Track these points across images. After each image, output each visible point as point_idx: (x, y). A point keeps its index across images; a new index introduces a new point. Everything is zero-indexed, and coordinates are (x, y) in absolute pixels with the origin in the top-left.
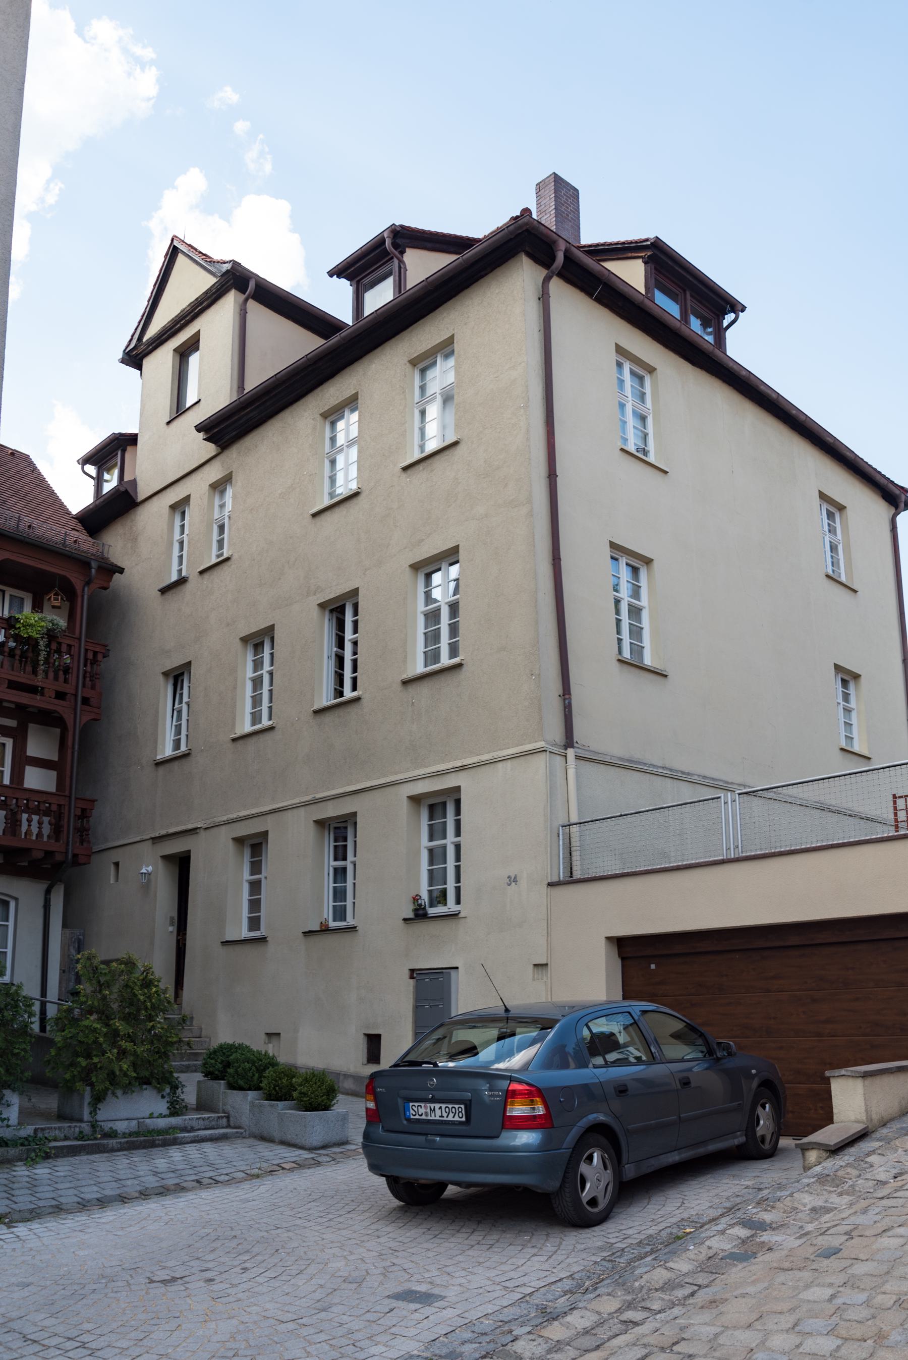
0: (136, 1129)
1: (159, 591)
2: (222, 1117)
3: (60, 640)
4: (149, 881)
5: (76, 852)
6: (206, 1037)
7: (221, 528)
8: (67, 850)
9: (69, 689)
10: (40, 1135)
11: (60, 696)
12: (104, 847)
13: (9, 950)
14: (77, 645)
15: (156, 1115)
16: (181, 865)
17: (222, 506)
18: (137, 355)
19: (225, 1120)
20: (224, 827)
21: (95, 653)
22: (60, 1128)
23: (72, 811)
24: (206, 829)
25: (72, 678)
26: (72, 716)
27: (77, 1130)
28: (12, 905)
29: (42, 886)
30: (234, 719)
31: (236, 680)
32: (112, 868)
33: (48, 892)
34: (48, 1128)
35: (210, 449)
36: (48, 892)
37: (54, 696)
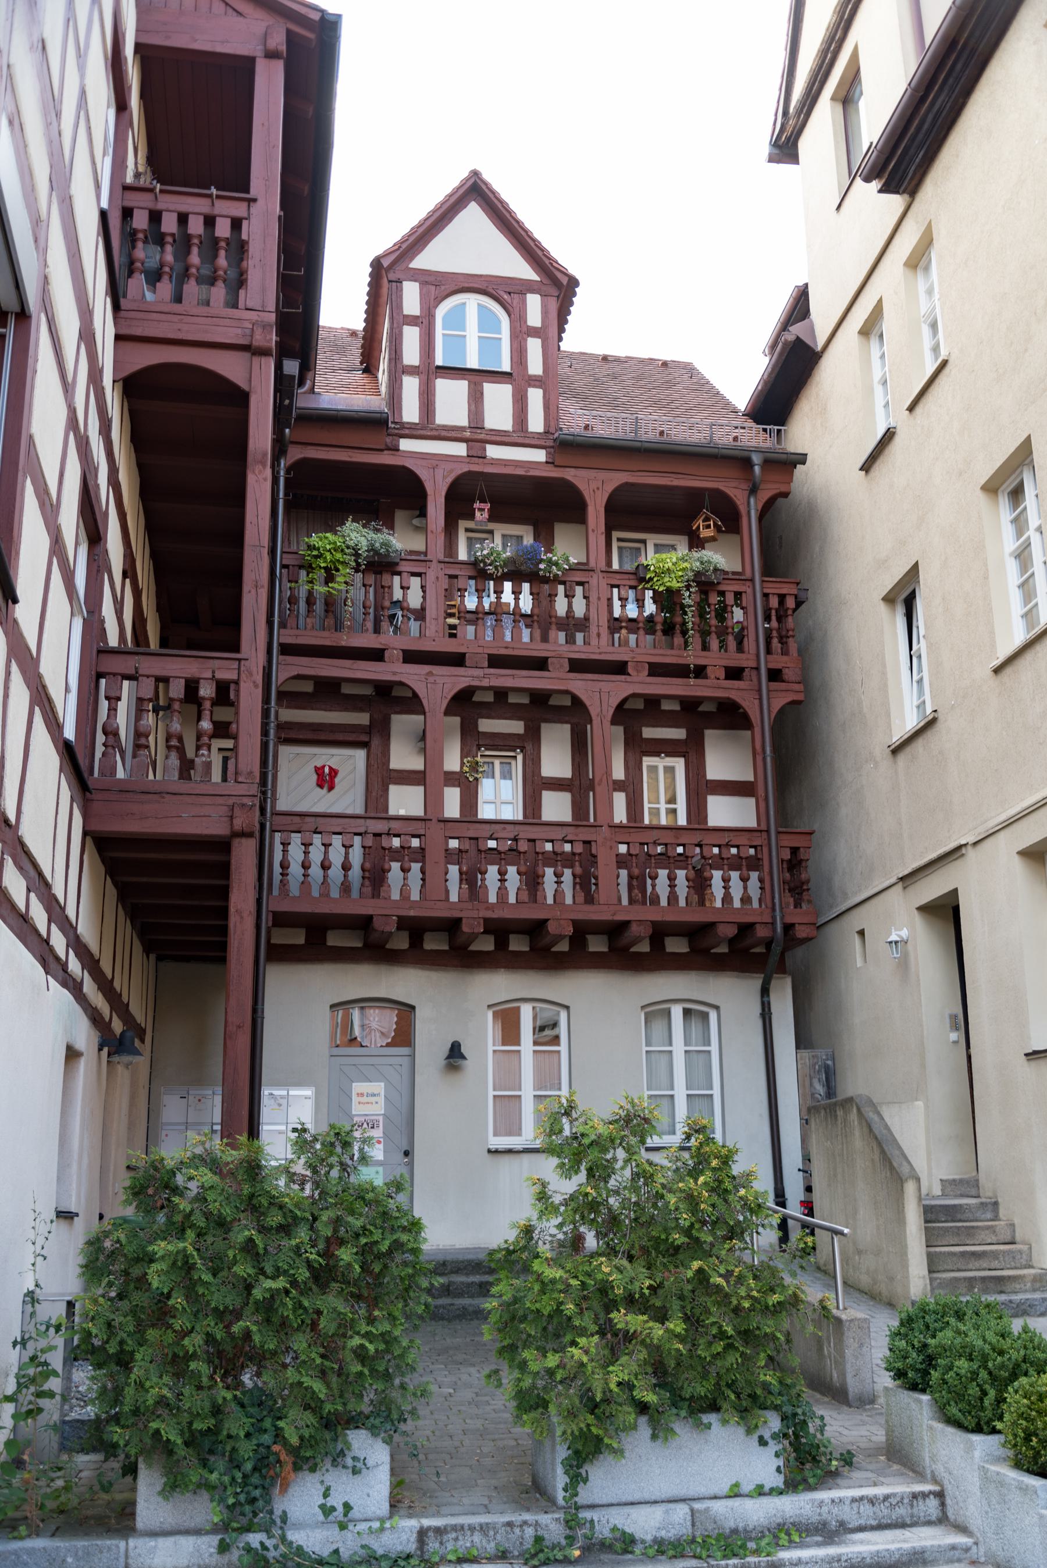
0: (686, 1530)
1: (861, 469)
2: (925, 1495)
3: (721, 588)
4: (905, 956)
5: (789, 920)
6: (1024, 1243)
7: (934, 326)
8: (774, 917)
9: (744, 660)
10: (432, 1545)
11: (734, 673)
12: (843, 908)
13: (716, 1092)
14: (749, 591)
15: (747, 1487)
16: (947, 913)
17: (930, 292)
18: (788, 139)
19: (933, 1503)
20: (1002, 834)
21: (782, 598)
22: (483, 1529)
23: (774, 853)
24: (975, 844)
25: (749, 643)
26: (757, 702)
27: (530, 1532)
28: (713, 1016)
29: (755, 983)
30: (992, 633)
31: (986, 565)
32: (857, 939)
33: (765, 991)
34: (454, 1528)
35: (895, 202)
36: (765, 991)
37: (723, 675)
